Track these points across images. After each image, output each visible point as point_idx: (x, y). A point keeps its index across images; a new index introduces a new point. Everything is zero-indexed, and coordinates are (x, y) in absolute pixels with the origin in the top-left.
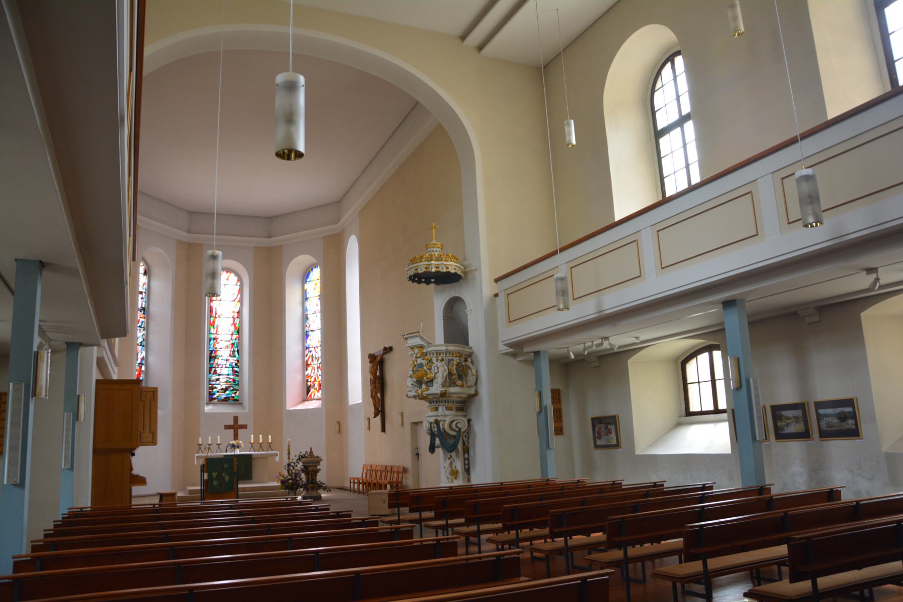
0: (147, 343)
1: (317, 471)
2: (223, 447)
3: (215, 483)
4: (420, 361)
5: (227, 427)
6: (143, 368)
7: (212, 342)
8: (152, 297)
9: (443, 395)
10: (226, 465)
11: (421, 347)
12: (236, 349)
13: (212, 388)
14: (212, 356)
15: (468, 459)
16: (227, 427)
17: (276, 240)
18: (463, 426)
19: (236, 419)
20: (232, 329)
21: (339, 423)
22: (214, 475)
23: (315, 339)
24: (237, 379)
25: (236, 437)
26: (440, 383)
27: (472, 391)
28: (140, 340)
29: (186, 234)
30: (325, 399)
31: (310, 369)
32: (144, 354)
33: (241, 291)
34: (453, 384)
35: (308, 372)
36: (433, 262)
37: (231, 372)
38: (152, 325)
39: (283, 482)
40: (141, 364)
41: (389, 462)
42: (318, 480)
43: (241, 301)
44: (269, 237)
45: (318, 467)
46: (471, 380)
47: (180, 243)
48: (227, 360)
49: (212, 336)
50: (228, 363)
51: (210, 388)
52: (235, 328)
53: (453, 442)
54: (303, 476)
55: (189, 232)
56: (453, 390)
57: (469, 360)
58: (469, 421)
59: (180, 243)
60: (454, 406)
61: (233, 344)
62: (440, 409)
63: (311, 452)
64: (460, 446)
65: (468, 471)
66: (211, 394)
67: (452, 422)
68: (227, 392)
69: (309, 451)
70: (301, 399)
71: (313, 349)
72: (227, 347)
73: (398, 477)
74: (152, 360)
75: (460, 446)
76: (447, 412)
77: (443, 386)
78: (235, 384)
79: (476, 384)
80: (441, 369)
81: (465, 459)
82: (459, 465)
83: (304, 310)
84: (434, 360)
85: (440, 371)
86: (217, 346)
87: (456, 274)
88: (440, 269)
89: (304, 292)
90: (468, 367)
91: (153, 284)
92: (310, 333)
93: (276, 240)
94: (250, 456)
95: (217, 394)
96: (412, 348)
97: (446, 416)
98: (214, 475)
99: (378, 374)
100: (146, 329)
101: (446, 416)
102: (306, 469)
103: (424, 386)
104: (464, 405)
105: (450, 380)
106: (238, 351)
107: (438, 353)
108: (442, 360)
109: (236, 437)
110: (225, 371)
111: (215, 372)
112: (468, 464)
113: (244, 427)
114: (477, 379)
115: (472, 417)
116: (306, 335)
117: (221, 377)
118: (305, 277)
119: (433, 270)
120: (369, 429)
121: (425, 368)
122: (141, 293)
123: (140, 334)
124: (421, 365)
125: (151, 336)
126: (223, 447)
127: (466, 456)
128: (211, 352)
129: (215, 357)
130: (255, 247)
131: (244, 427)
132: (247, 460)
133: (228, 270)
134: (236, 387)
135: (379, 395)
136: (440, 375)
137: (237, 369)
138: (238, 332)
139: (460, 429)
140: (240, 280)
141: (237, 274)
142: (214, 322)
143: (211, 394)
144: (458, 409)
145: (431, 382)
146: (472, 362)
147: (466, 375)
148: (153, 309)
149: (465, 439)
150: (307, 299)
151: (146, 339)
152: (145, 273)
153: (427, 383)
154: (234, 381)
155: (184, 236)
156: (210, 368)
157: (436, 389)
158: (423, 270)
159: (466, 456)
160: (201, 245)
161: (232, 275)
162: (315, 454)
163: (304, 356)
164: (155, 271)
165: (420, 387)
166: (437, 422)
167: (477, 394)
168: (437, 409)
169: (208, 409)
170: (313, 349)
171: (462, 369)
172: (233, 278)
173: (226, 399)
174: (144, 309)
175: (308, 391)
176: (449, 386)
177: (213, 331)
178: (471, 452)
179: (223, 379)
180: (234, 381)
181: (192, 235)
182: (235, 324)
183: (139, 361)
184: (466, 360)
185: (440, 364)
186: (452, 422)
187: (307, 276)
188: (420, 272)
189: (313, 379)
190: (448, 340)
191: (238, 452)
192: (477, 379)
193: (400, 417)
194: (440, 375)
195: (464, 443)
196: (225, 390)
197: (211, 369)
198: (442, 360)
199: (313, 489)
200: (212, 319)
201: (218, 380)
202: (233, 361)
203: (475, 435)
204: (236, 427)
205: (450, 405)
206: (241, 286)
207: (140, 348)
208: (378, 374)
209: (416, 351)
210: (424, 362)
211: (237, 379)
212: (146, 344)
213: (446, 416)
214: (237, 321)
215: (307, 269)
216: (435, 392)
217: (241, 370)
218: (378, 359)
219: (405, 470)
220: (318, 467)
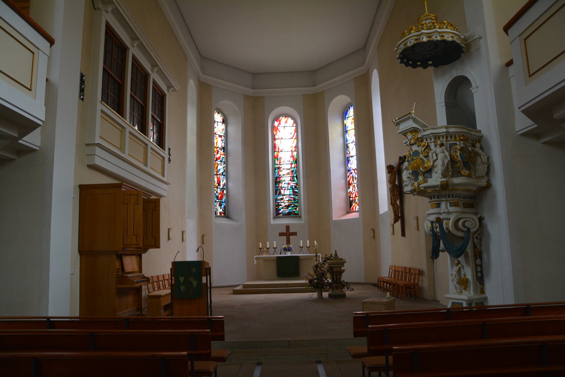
0: (227, 173)
1: (341, 272)
2: (278, 250)
3: (182, 288)
4: (415, 148)
5: (281, 234)
6: (225, 192)
7: (276, 171)
8: (229, 139)
9: (444, 186)
10: (194, 270)
11: (415, 131)
12: (295, 175)
13: (278, 205)
14: (277, 181)
15: (481, 266)
16: (281, 234)
17: (319, 88)
18: (472, 223)
19: (288, 227)
20: (292, 160)
21: (373, 230)
22: (182, 279)
23: (353, 164)
24: (297, 198)
25: (288, 242)
26: (440, 172)
27: (483, 183)
28: (221, 171)
29: (252, 90)
30: (361, 211)
31: (351, 187)
32: (225, 181)
33: (296, 131)
34: (456, 173)
35: (351, 189)
36: (423, 31)
37: (292, 193)
38: (230, 159)
39: (310, 281)
40: (223, 189)
41: (408, 265)
42: (342, 280)
43: (297, 138)
44: (314, 86)
45: (343, 268)
46: (481, 169)
47: (246, 97)
48: (288, 184)
49: (276, 166)
50: (289, 186)
51: (276, 206)
52: (294, 159)
53: (463, 244)
54: (328, 275)
55: (253, 88)
56: (457, 180)
57: (478, 145)
58: (481, 219)
59: (246, 97)
60: (461, 204)
61: (292, 171)
62: (443, 205)
63: (336, 255)
64: (469, 249)
65: (480, 279)
66: (277, 211)
67: (458, 220)
68: (290, 208)
69: (333, 254)
70: (344, 212)
71: (353, 171)
72: (288, 174)
73: (415, 279)
74: (230, 185)
75: (469, 249)
76: (452, 209)
77: (444, 175)
78: (295, 202)
79: (488, 173)
80: (440, 156)
81: (476, 266)
82: (468, 273)
83: (345, 141)
84: (432, 146)
85: (439, 158)
86: (280, 173)
87: (453, 42)
88: (434, 38)
89: (344, 127)
90: (477, 154)
91: (230, 129)
92: (350, 158)
93: (319, 88)
94: (298, 257)
95: (282, 210)
96: (405, 133)
97: (450, 213)
98: (182, 279)
99: (397, 183)
100: (226, 163)
101: (449, 213)
102: (331, 270)
103: (421, 178)
104: (475, 199)
105: (452, 168)
106: (296, 177)
107: (436, 137)
108: (442, 145)
109: (288, 242)
110: (287, 192)
111: (280, 193)
112: (481, 272)
113: (295, 234)
114: (488, 168)
115: (485, 215)
116: (347, 160)
117: (285, 197)
118: (344, 115)
119: (425, 39)
120: (393, 234)
121: (421, 156)
122: (220, 136)
123: (221, 168)
124: (416, 153)
125: (230, 168)
126: (278, 250)
127: (478, 262)
128: (277, 178)
129: (279, 182)
130: (303, 95)
131: (295, 234)
132: (296, 259)
133: (286, 116)
134: (296, 204)
135: (398, 202)
136: (439, 163)
137: (296, 190)
138: (296, 162)
139: (469, 229)
140: (295, 122)
141: (293, 118)
142: (278, 155)
143: (277, 211)
144: (466, 206)
145: (429, 171)
146: (482, 148)
147: (474, 163)
148: (230, 147)
149: (476, 241)
150: (346, 132)
151: (226, 170)
152: (223, 122)
153: (424, 173)
154: (294, 199)
155: (250, 92)
156: (276, 191)
157: (436, 179)
158: (413, 42)
159: (478, 262)
160: (262, 97)
161: (289, 119)
162: (340, 256)
163: (346, 177)
164: (230, 120)
165: (416, 179)
166: (439, 221)
167: (489, 186)
168: (438, 206)
169: (273, 222)
170: (353, 171)
171: (469, 154)
172: (290, 121)
173: (289, 214)
174: (223, 148)
175: (351, 205)
176: (453, 176)
177: (277, 162)
178: (485, 256)
179: (286, 199)
180: (294, 199)
181: (255, 90)
182: (293, 156)
183: (221, 187)
184: (474, 146)
185: (438, 150)
186: (458, 220)
187: (346, 114)
188: (409, 45)
189: (354, 196)
190: (450, 120)
191: (289, 254)
192: (488, 168)
193: (416, 222)
194: (439, 163)
195: (475, 246)
196: (288, 207)
197: (277, 191)
198: (442, 145)
199: (337, 288)
200: (276, 153)
201: (282, 199)
202: (292, 184)
203: (489, 236)
204: (288, 234)
205: (456, 200)
206: (297, 127)
207: (222, 177)
208: (397, 183)
209: (410, 136)
210: (420, 149)
211: (297, 198)
212: (226, 174)
213: (449, 213)
214: (295, 153)
215: (346, 107)
216: (435, 183)
217: (299, 191)
218: (395, 170)
219: (421, 273)
220: (343, 268)
